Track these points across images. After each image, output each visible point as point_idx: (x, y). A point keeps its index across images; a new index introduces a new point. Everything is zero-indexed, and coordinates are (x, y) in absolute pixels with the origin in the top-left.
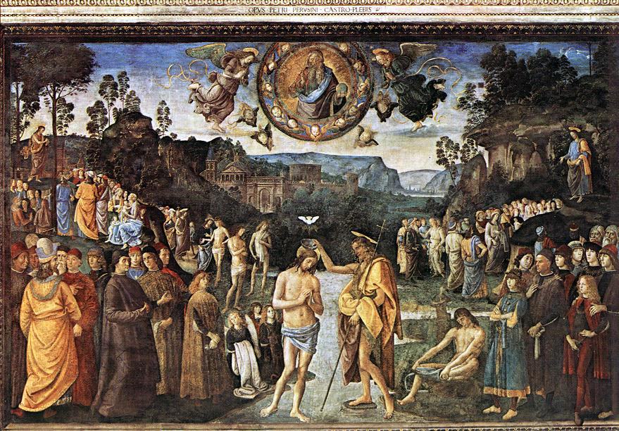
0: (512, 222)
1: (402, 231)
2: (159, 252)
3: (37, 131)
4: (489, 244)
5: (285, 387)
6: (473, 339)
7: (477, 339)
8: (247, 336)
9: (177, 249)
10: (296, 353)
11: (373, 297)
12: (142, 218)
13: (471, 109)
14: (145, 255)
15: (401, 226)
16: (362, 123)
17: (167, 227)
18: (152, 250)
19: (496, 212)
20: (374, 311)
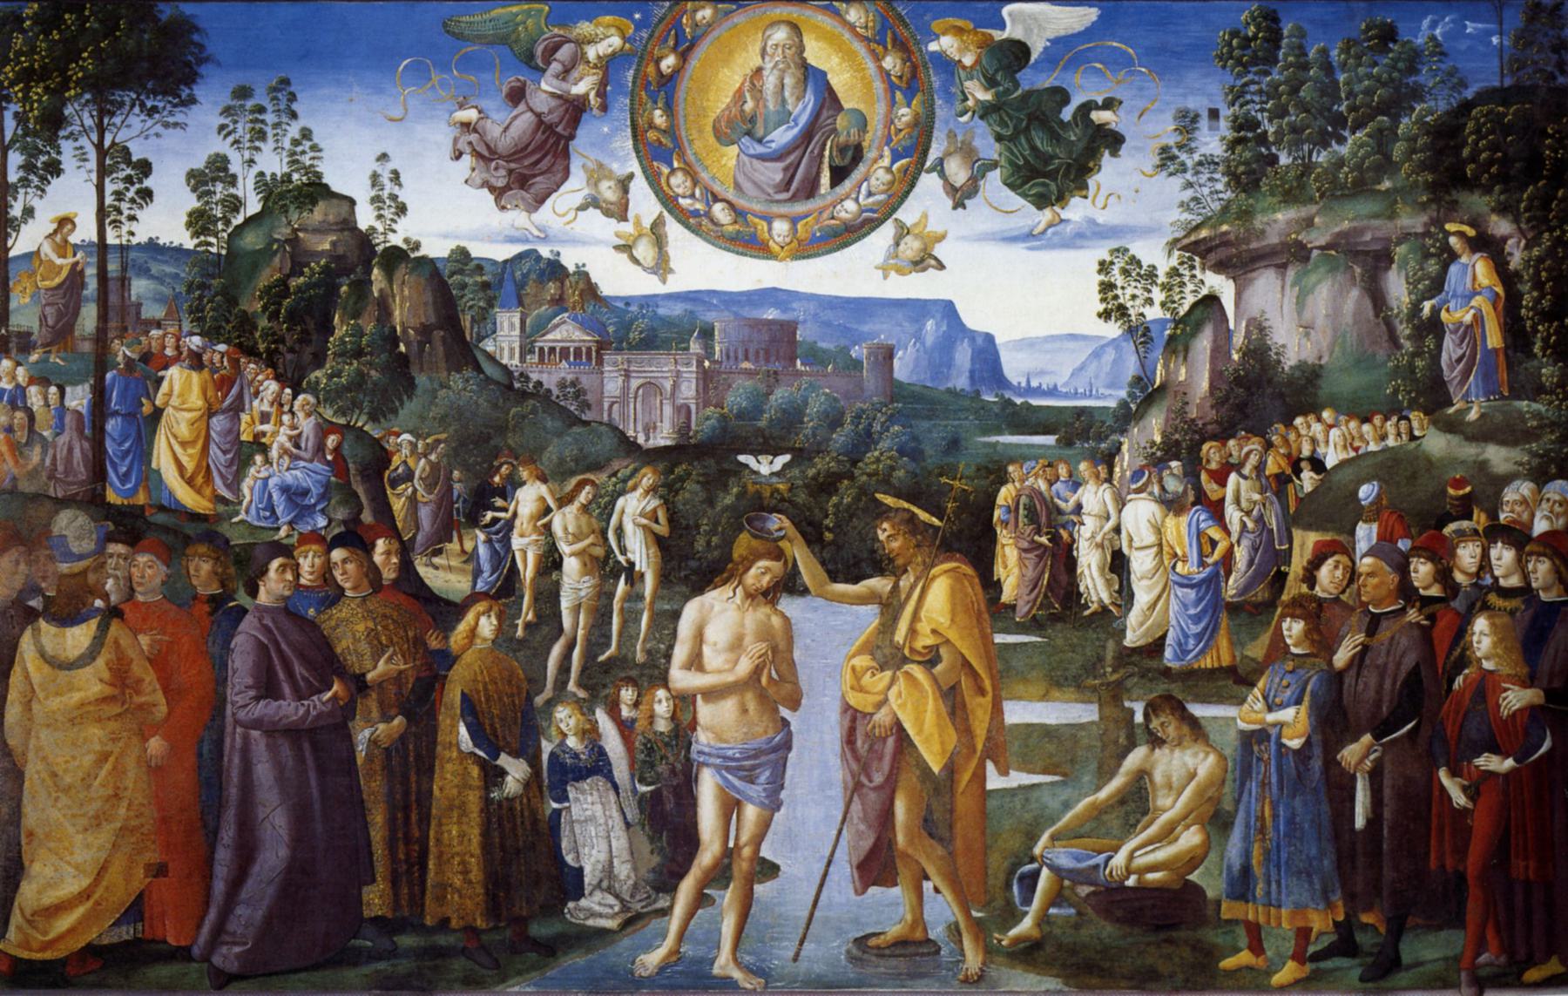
0: (1297, 471)
1: (1005, 494)
2: (373, 545)
3: (56, 232)
4: (1235, 528)
5: (701, 900)
6: (1193, 776)
7: (1203, 772)
8: (598, 765)
9: (419, 537)
10: (730, 807)
11: (931, 660)
12: (329, 458)
13: (1188, 176)
14: (337, 555)
15: (1003, 479)
16: (908, 213)
17: (394, 483)
18: (355, 539)
19: (1255, 445)
20: (932, 706)
